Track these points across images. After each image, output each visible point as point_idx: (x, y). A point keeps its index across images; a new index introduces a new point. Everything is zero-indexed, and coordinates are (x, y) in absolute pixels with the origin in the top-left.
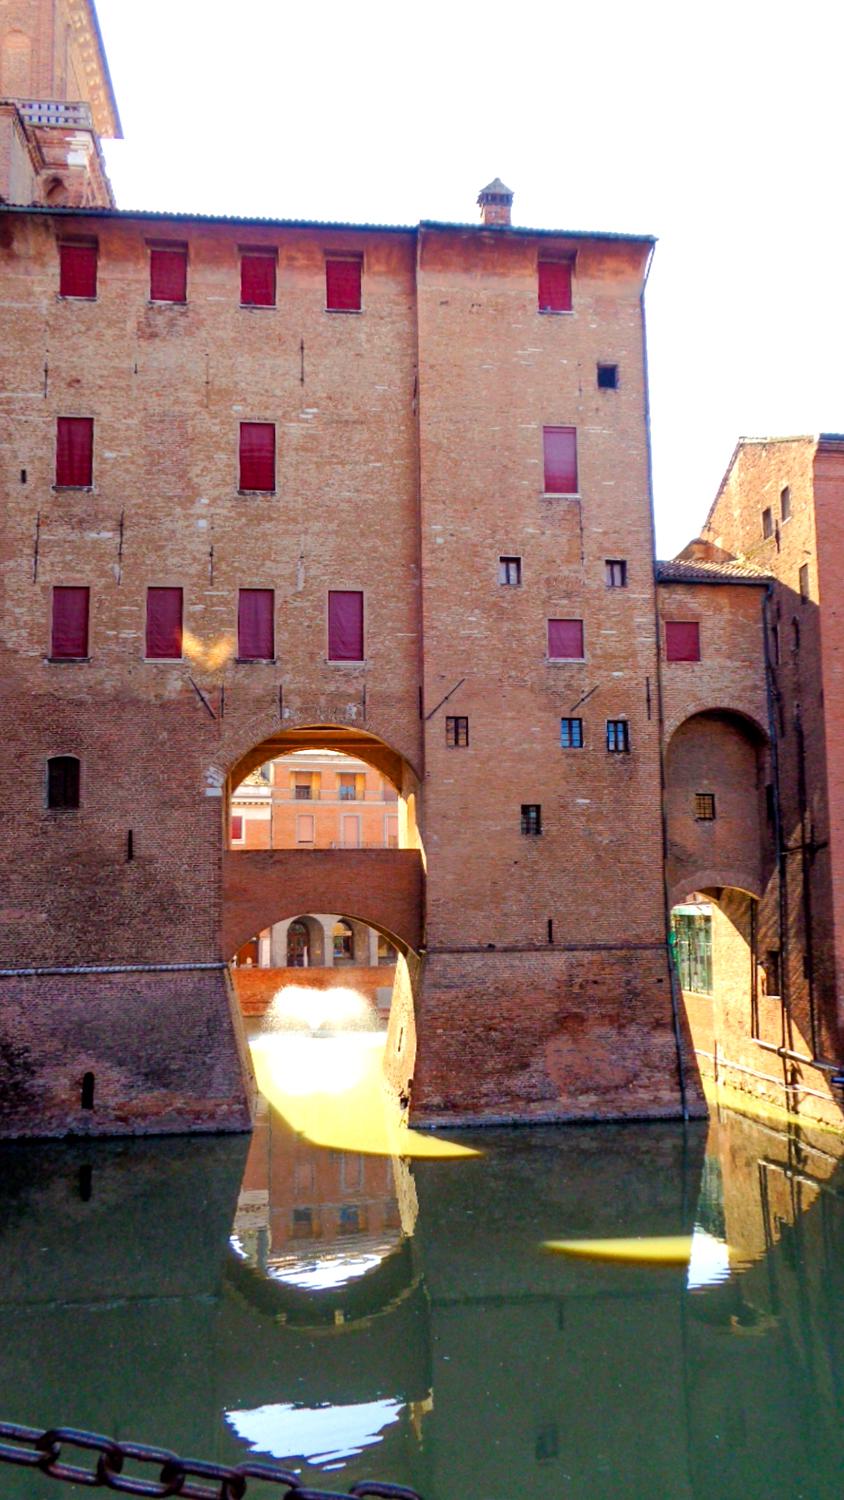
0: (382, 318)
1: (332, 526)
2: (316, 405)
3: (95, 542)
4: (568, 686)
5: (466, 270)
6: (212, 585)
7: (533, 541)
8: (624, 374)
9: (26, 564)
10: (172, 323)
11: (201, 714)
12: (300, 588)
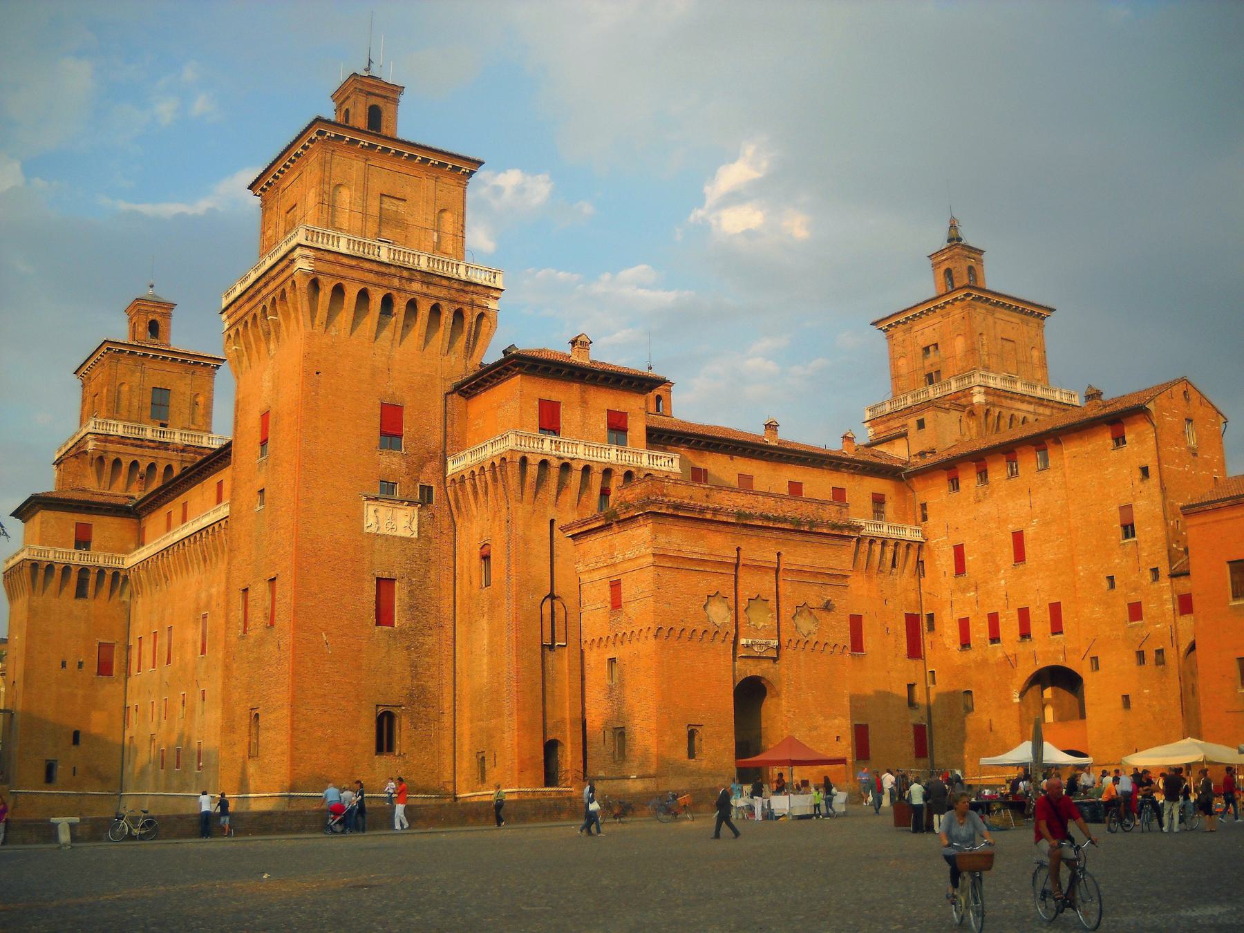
0: (1057, 468)
1: (1048, 573)
2: (1037, 517)
4: (1137, 635)
5: (1081, 438)
7: (1118, 566)
8: (1153, 470)
10: (985, 494)
11: (1010, 666)
12: (1038, 605)
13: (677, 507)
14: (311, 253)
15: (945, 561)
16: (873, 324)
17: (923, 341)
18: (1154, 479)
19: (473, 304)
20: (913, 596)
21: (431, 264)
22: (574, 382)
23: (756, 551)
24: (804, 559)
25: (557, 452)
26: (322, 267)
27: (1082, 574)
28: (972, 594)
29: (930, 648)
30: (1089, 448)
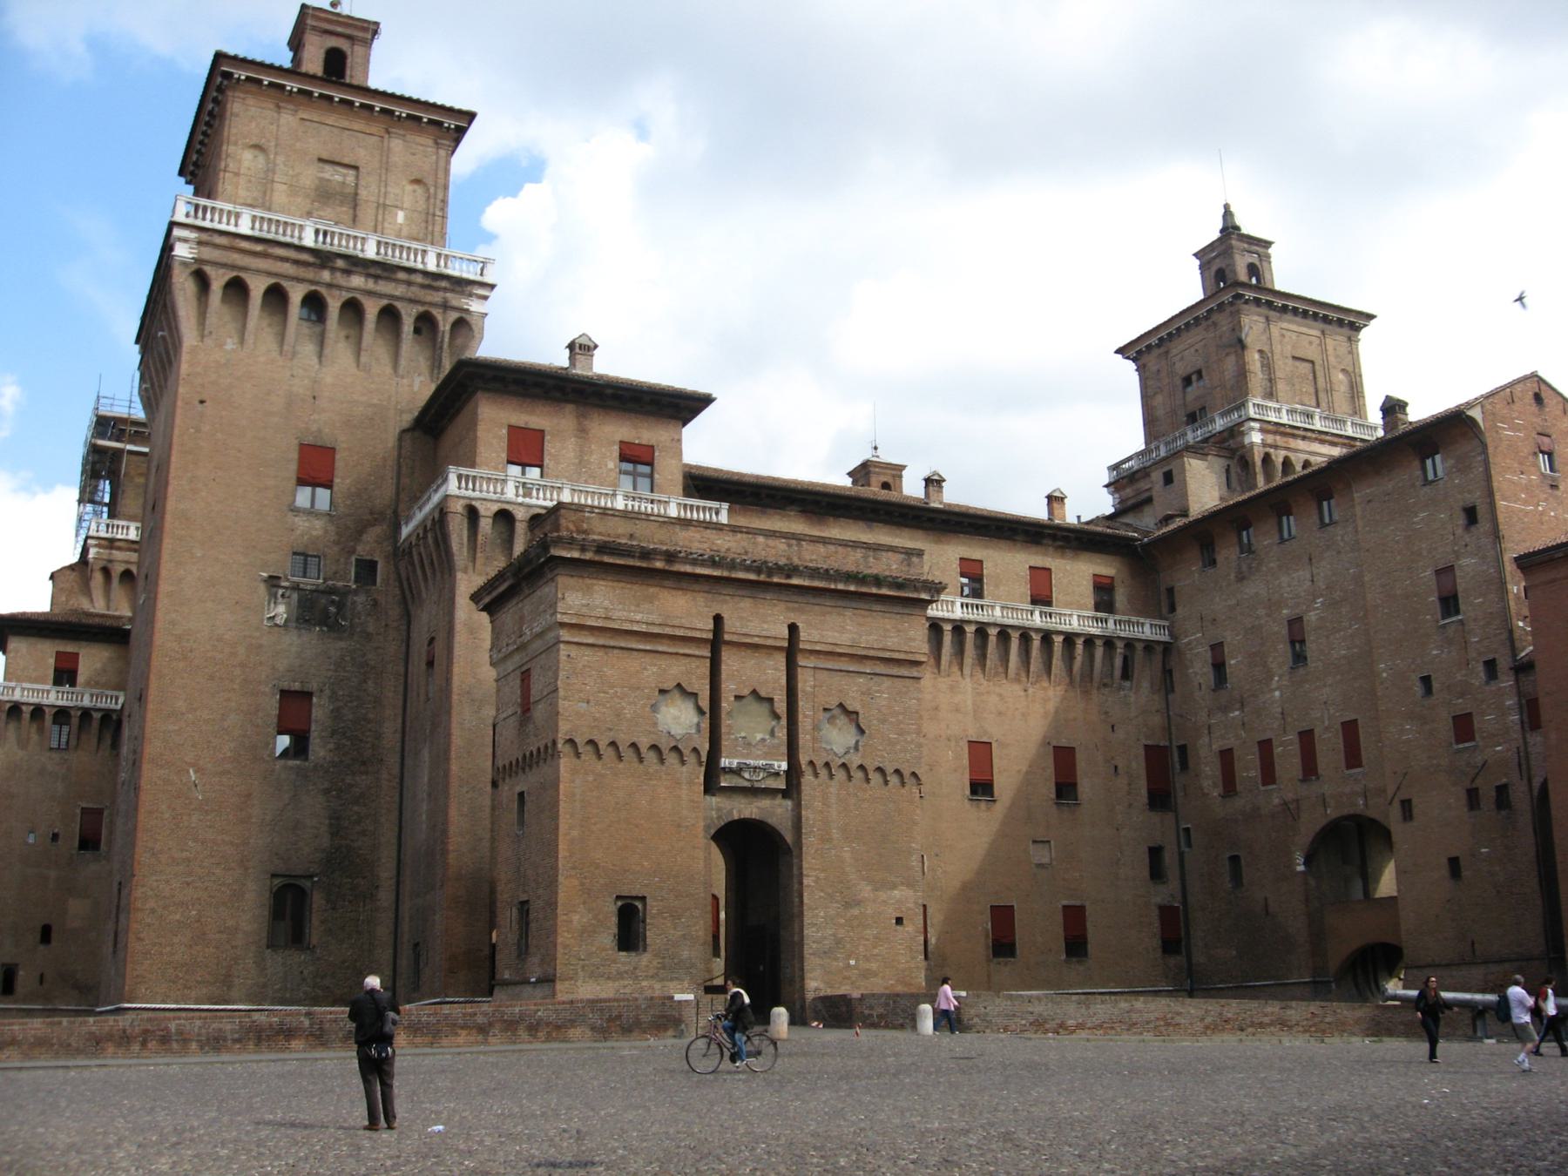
0: (1347, 521)
2: (1322, 596)
3: (1233, 718)
6: (1285, 732)
8: (1482, 511)
9: (1207, 740)
10: (1250, 568)
12: (1327, 723)
13: (602, 548)
14: (193, 235)
15: (1199, 670)
16: (1118, 351)
17: (1182, 369)
18: (1484, 526)
19: (446, 306)
20: (1157, 720)
21: (382, 251)
22: (568, 401)
23: (749, 621)
24: (836, 634)
25: (527, 500)
26: (208, 253)
27: (1385, 675)
28: (1237, 713)
29: (1182, 794)
30: (1390, 486)
